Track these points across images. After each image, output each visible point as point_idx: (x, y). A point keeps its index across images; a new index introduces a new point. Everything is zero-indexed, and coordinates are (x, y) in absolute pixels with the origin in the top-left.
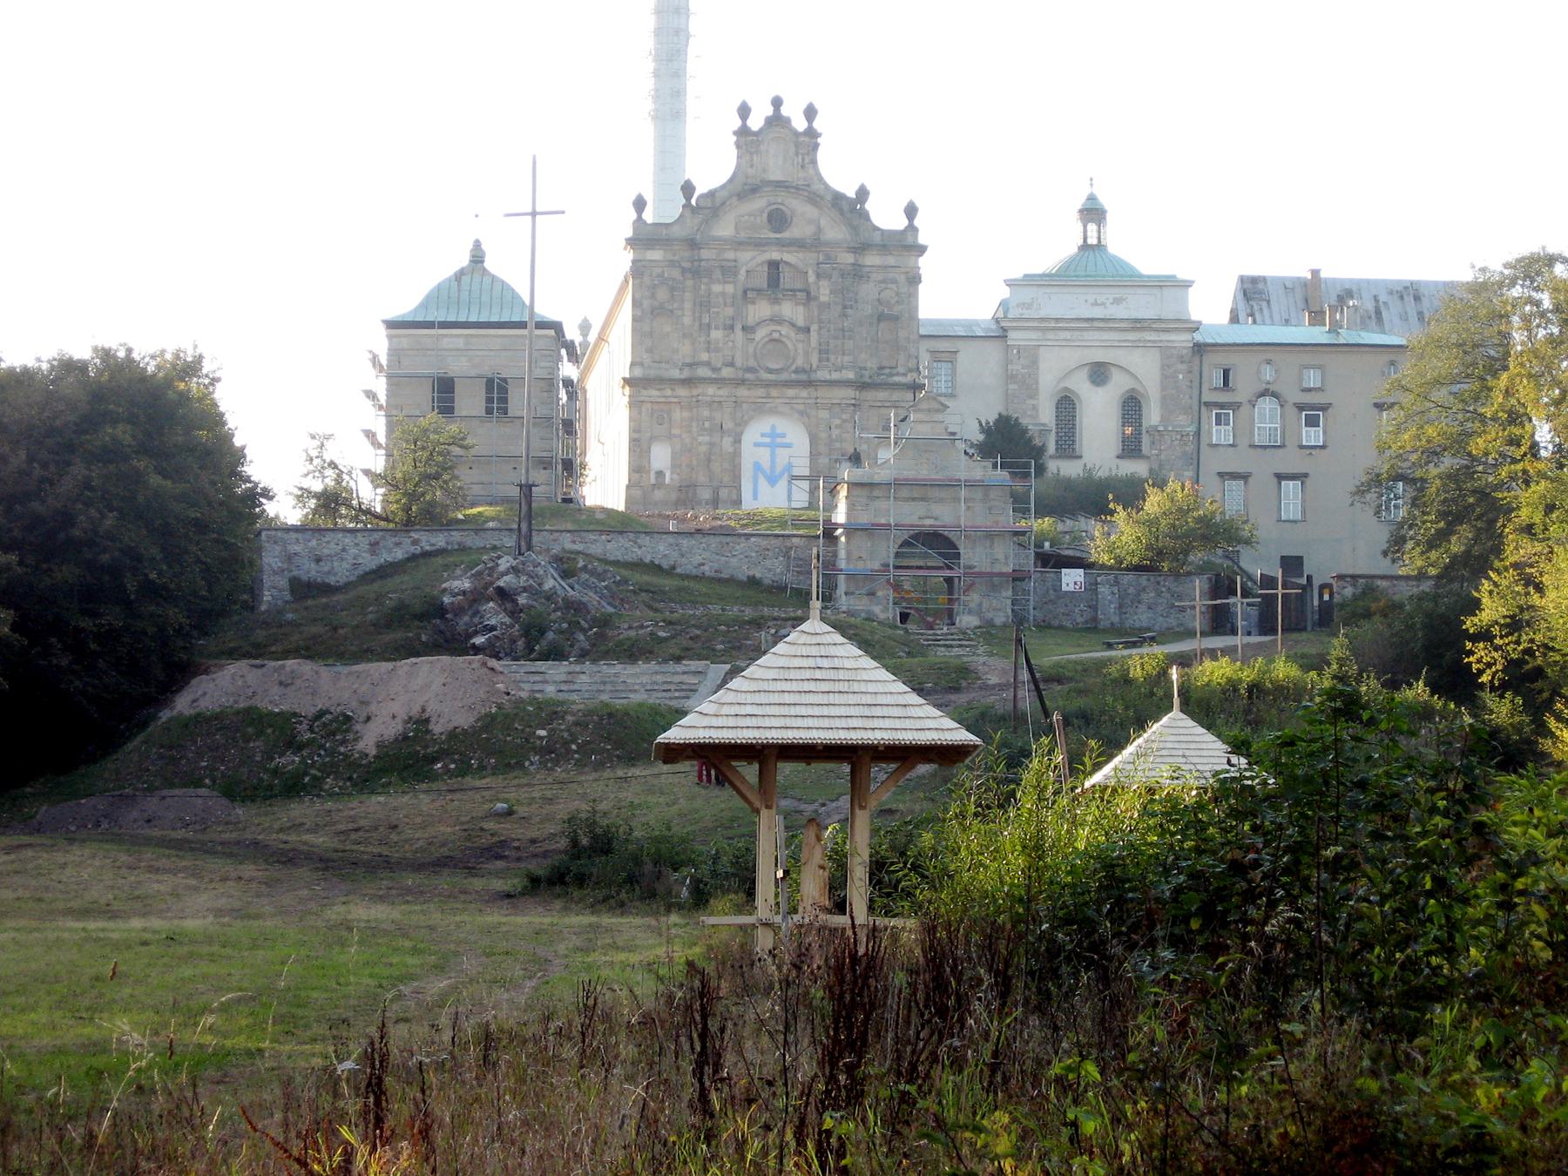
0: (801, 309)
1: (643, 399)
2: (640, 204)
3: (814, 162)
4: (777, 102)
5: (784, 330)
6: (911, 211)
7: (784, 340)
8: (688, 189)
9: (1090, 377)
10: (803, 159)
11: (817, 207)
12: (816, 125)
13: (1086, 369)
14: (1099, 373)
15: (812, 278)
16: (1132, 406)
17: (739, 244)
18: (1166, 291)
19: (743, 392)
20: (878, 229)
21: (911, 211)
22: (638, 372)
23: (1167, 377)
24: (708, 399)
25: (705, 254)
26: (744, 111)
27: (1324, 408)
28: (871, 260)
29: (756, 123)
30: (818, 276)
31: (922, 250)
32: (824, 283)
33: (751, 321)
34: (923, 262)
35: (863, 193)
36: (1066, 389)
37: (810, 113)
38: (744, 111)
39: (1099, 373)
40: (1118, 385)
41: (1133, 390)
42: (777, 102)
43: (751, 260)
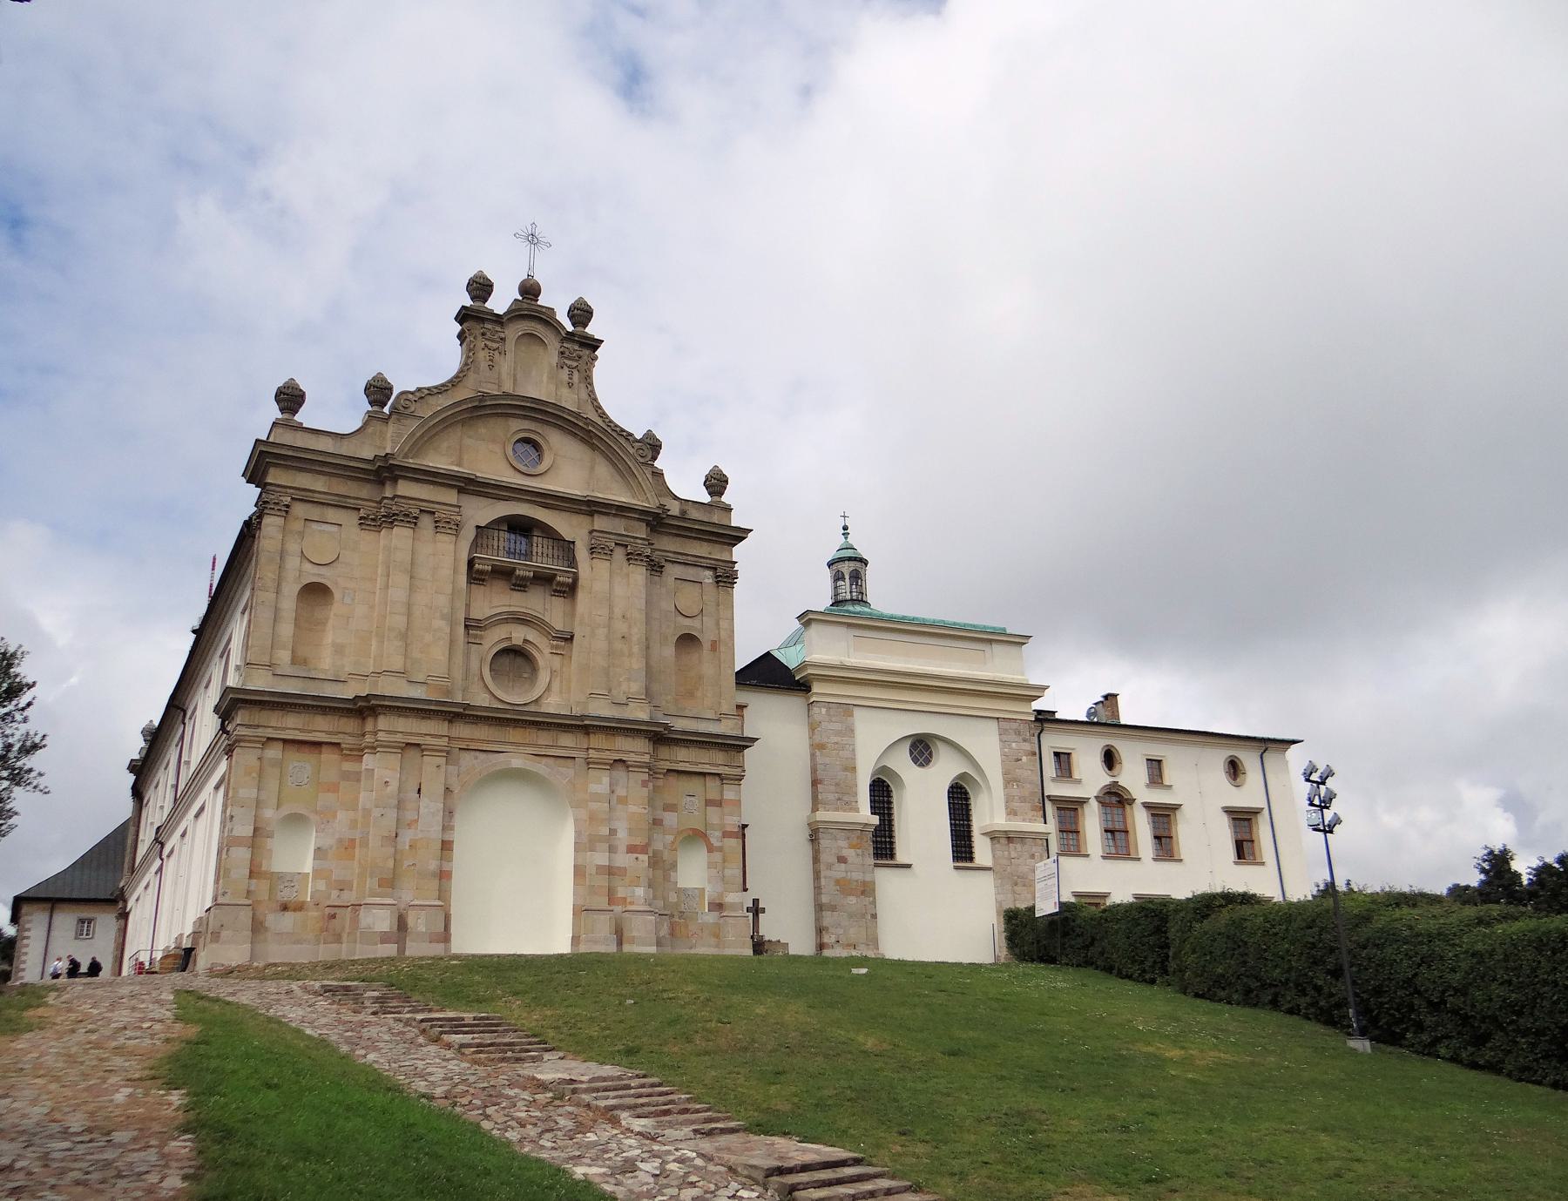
0: (558, 604)
1: (271, 733)
2: (290, 398)
3: (588, 380)
4: (530, 290)
5: (532, 635)
6: (717, 482)
7: (528, 647)
8: (378, 391)
9: (911, 753)
10: (571, 374)
11: (593, 447)
12: (592, 329)
13: (907, 746)
14: (922, 748)
15: (582, 553)
16: (959, 799)
17: (469, 486)
18: (997, 648)
19: (463, 731)
20: (676, 498)
21: (717, 482)
22: (260, 682)
23: (1010, 763)
24: (399, 738)
25: (405, 488)
26: (481, 288)
27: (1175, 808)
28: (668, 544)
29: (499, 303)
30: (592, 550)
31: (739, 535)
32: (602, 566)
33: (477, 614)
34: (739, 552)
35: (652, 446)
36: (884, 769)
37: (581, 313)
38: (481, 288)
39: (922, 748)
40: (944, 770)
41: (963, 776)
42: (530, 290)
43: (483, 512)
